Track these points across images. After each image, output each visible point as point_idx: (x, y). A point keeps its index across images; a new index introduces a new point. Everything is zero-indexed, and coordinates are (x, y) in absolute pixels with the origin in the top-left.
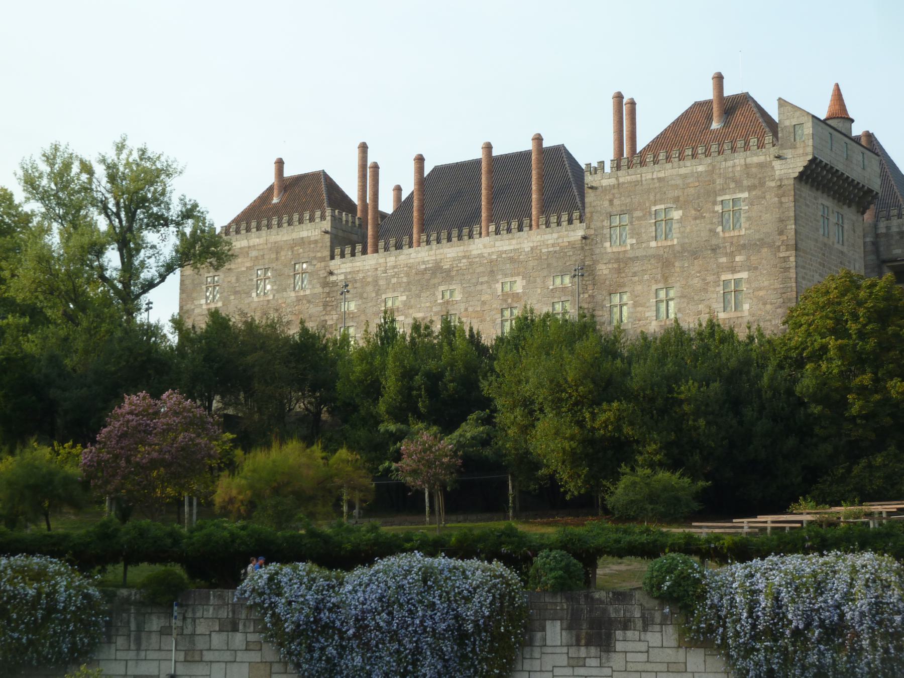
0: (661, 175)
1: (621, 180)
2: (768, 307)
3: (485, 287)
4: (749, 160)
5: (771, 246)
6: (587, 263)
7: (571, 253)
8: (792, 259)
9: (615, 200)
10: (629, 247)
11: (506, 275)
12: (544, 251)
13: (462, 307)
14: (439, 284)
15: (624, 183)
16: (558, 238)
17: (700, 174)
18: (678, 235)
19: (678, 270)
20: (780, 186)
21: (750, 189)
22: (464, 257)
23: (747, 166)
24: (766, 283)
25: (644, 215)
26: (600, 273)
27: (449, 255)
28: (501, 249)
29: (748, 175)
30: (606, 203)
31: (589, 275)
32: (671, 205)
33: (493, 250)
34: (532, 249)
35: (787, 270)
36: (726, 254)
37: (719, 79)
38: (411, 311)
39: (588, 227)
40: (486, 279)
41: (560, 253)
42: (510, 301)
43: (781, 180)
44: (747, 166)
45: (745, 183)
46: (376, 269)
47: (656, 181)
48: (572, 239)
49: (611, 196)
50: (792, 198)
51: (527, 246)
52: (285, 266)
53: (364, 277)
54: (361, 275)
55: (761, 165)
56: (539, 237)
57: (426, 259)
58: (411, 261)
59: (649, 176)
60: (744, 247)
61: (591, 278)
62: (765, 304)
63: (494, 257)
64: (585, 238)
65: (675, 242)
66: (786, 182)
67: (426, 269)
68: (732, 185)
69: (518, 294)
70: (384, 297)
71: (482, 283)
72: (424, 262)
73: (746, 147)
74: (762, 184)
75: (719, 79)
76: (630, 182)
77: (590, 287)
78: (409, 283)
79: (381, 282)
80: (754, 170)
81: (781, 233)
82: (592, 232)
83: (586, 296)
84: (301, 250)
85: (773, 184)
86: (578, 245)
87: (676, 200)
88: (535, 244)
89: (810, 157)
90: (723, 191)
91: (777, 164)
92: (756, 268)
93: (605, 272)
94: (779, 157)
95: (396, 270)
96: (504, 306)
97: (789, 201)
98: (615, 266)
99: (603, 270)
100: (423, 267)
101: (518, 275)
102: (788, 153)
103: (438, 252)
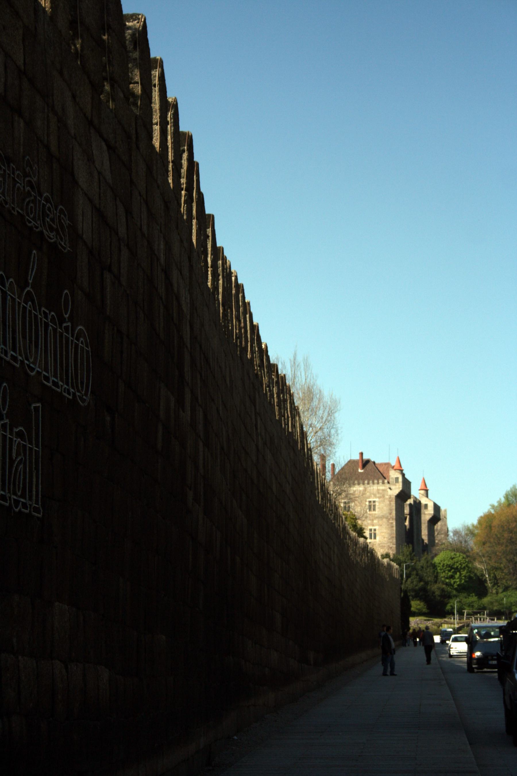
2: (385, 539)
4: (379, 488)
5: (387, 518)
8: (394, 523)
17: (360, 491)
20: (390, 498)
21: (379, 498)
23: (378, 490)
24: (385, 531)
29: (378, 493)
35: (392, 527)
36: (370, 520)
37: (362, 454)
43: (390, 496)
44: (378, 490)
45: (378, 495)
50: (394, 502)
55: (383, 490)
60: (377, 518)
62: (384, 538)
66: (392, 497)
68: (373, 496)
73: (378, 483)
74: (383, 496)
75: (362, 454)
80: (381, 491)
81: (390, 514)
85: (387, 497)
89: (401, 489)
90: (369, 497)
91: (389, 490)
92: (381, 525)
94: (390, 489)
97: (393, 504)
102: (393, 487)
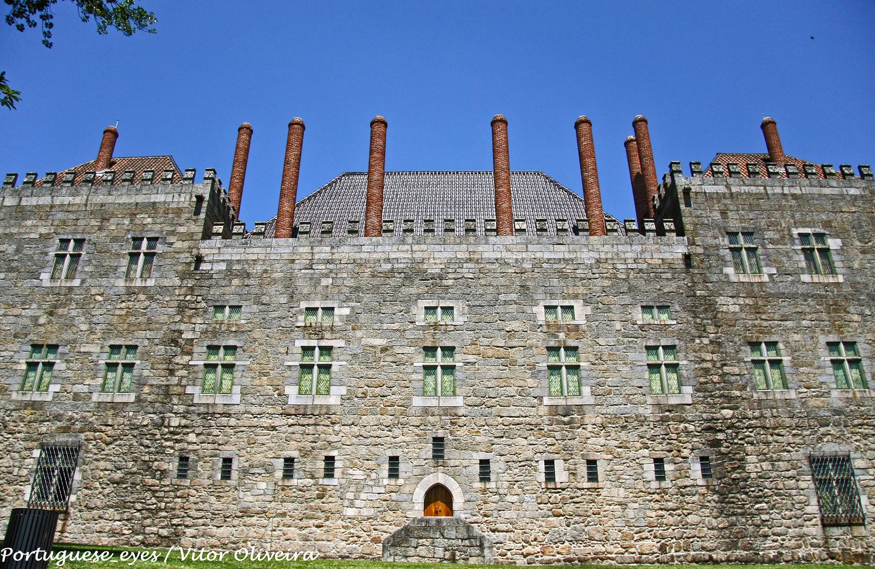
0: (797, 191)
1: (734, 189)
3: (513, 308)
6: (698, 293)
7: (669, 275)
9: (730, 214)
10: (766, 278)
11: (552, 295)
12: (619, 266)
13: (468, 336)
14: (419, 297)
15: (740, 194)
16: (643, 252)
18: (844, 271)
19: (856, 317)
22: (470, 260)
25: (783, 237)
26: (725, 308)
27: (437, 255)
28: (539, 255)
30: (717, 215)
31: (706, 310)
32: (822, 231)
33: (524, 255)
34: (598, 261)
38: (359, 334)
39: (692, 243)
40: (514, 296)
41: (653, 274)
42: (562, 336)
46: (293, 261)
47: (790, 198)
48: (667, 256)
49: (722, 207)
51: (587, 256)
52: (115, 239)
53: (266, 271)
54: (259, 268)
56: (607, 248)
57: (392, 256)
58: (363, 256)
59: (778, 190)
61: (710, 315)
63: (527, 266)
64: (687, 258)
65: (841, 279)
67: (392, 271)
69: (577, 326)
70: (304, 305)
71: (506, 302)
72: (388, 260)
76: (750, 194)
77: (711, 329)
78: (357, 289)
79: (299, 283)
82: (700, 250)
83: (706, 341)
84: (150, 220)
86: (680, 265)
87: (827, 224)
88: (603, 256)
93: (732, 308)
95: (331, 266)
96: (552, 344)
98: (749, 301)
99: (728, 305)
100: (389, 266)
101: (576, 297)
103: (415, 248)
